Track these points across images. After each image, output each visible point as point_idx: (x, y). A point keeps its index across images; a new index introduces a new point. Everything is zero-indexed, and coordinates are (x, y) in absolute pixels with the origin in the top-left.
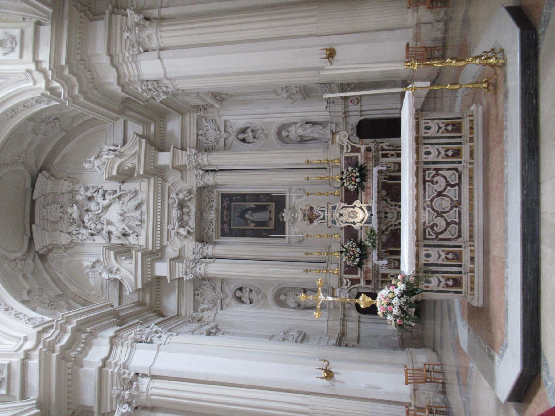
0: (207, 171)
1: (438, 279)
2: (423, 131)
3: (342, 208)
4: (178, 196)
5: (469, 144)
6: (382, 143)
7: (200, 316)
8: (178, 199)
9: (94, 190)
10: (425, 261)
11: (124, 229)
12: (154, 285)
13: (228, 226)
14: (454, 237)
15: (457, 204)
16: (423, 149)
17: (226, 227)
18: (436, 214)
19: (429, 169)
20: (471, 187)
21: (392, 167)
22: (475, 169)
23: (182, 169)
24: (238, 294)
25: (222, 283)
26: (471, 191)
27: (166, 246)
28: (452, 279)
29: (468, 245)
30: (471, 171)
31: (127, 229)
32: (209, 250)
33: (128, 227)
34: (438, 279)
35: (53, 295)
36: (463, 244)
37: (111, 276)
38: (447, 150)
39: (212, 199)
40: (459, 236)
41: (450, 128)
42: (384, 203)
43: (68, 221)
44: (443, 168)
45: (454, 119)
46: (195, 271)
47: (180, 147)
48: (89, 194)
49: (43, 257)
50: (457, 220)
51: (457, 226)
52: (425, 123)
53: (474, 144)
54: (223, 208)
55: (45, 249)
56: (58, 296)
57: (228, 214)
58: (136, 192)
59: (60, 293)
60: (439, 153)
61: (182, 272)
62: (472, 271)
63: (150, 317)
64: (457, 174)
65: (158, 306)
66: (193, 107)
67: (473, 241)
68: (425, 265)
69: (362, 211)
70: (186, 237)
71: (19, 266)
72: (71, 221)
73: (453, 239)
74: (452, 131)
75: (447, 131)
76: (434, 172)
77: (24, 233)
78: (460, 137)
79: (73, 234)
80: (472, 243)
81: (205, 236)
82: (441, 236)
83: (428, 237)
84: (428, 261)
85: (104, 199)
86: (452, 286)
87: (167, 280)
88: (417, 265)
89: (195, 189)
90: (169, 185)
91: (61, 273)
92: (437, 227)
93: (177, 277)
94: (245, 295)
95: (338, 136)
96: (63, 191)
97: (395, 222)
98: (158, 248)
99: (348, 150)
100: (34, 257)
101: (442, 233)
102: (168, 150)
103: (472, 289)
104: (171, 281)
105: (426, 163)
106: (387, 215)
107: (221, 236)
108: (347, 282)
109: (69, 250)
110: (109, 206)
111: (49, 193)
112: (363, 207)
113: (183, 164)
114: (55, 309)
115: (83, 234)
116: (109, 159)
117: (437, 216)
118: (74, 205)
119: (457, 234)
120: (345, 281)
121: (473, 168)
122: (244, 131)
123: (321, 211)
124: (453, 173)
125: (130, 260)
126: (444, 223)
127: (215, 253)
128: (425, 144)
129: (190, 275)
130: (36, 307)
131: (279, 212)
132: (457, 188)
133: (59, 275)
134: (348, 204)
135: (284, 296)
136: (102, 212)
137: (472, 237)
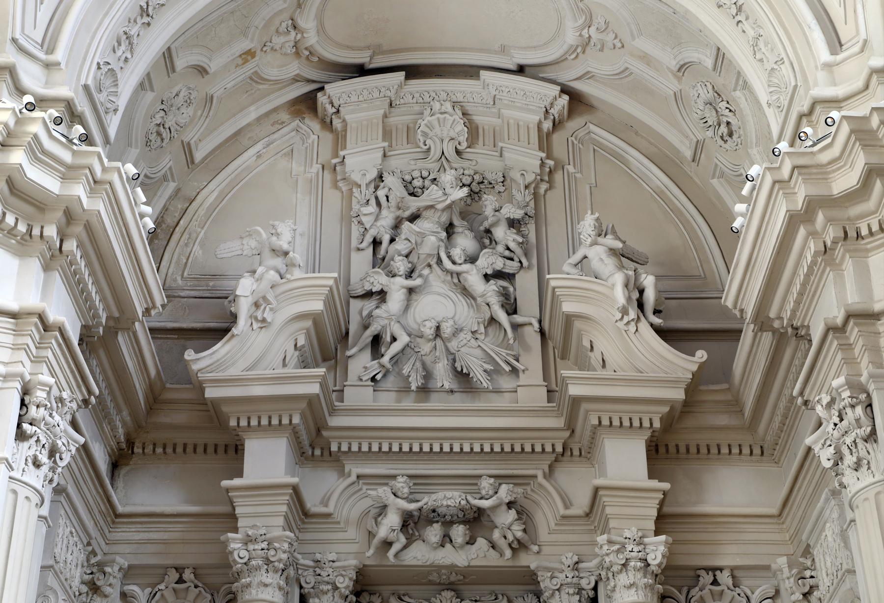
7: (108, 590)
9: (512, 245)
11: (394, 339)
12: (218, 440)
31: (396, 347)
33: (403, 350)
35: (189, 136)
43: (416, 174)
46: (258, 568)
48: (501, 233)
49: (307, 104)
55: (331, 110)
56: (188, 150)
58: (514, 371)
59: (198, 156)
61: (253, 527)
63: (113, 429)
65: (149, 449)
66: (807, 552)
70: (371, 535)
71: (278, 41)
77: (378, 50)
79: (376, 188)
87: (231, 478)
89: (528, 560)
90: (541, 479)
91: (259, 156)
93: (238, 511)
96: (506, 154)
98: (334, 448)
100: (309, 81)
102: (652, 474)
104: (228, 490)
109: (328, 176)
110: (466, 292)
113: (612, 524)
114: (148, 143)
115: (376, 220)
118: (466, 190)
129: (244, 553)
133: (252, 152)
136: (447, 271)
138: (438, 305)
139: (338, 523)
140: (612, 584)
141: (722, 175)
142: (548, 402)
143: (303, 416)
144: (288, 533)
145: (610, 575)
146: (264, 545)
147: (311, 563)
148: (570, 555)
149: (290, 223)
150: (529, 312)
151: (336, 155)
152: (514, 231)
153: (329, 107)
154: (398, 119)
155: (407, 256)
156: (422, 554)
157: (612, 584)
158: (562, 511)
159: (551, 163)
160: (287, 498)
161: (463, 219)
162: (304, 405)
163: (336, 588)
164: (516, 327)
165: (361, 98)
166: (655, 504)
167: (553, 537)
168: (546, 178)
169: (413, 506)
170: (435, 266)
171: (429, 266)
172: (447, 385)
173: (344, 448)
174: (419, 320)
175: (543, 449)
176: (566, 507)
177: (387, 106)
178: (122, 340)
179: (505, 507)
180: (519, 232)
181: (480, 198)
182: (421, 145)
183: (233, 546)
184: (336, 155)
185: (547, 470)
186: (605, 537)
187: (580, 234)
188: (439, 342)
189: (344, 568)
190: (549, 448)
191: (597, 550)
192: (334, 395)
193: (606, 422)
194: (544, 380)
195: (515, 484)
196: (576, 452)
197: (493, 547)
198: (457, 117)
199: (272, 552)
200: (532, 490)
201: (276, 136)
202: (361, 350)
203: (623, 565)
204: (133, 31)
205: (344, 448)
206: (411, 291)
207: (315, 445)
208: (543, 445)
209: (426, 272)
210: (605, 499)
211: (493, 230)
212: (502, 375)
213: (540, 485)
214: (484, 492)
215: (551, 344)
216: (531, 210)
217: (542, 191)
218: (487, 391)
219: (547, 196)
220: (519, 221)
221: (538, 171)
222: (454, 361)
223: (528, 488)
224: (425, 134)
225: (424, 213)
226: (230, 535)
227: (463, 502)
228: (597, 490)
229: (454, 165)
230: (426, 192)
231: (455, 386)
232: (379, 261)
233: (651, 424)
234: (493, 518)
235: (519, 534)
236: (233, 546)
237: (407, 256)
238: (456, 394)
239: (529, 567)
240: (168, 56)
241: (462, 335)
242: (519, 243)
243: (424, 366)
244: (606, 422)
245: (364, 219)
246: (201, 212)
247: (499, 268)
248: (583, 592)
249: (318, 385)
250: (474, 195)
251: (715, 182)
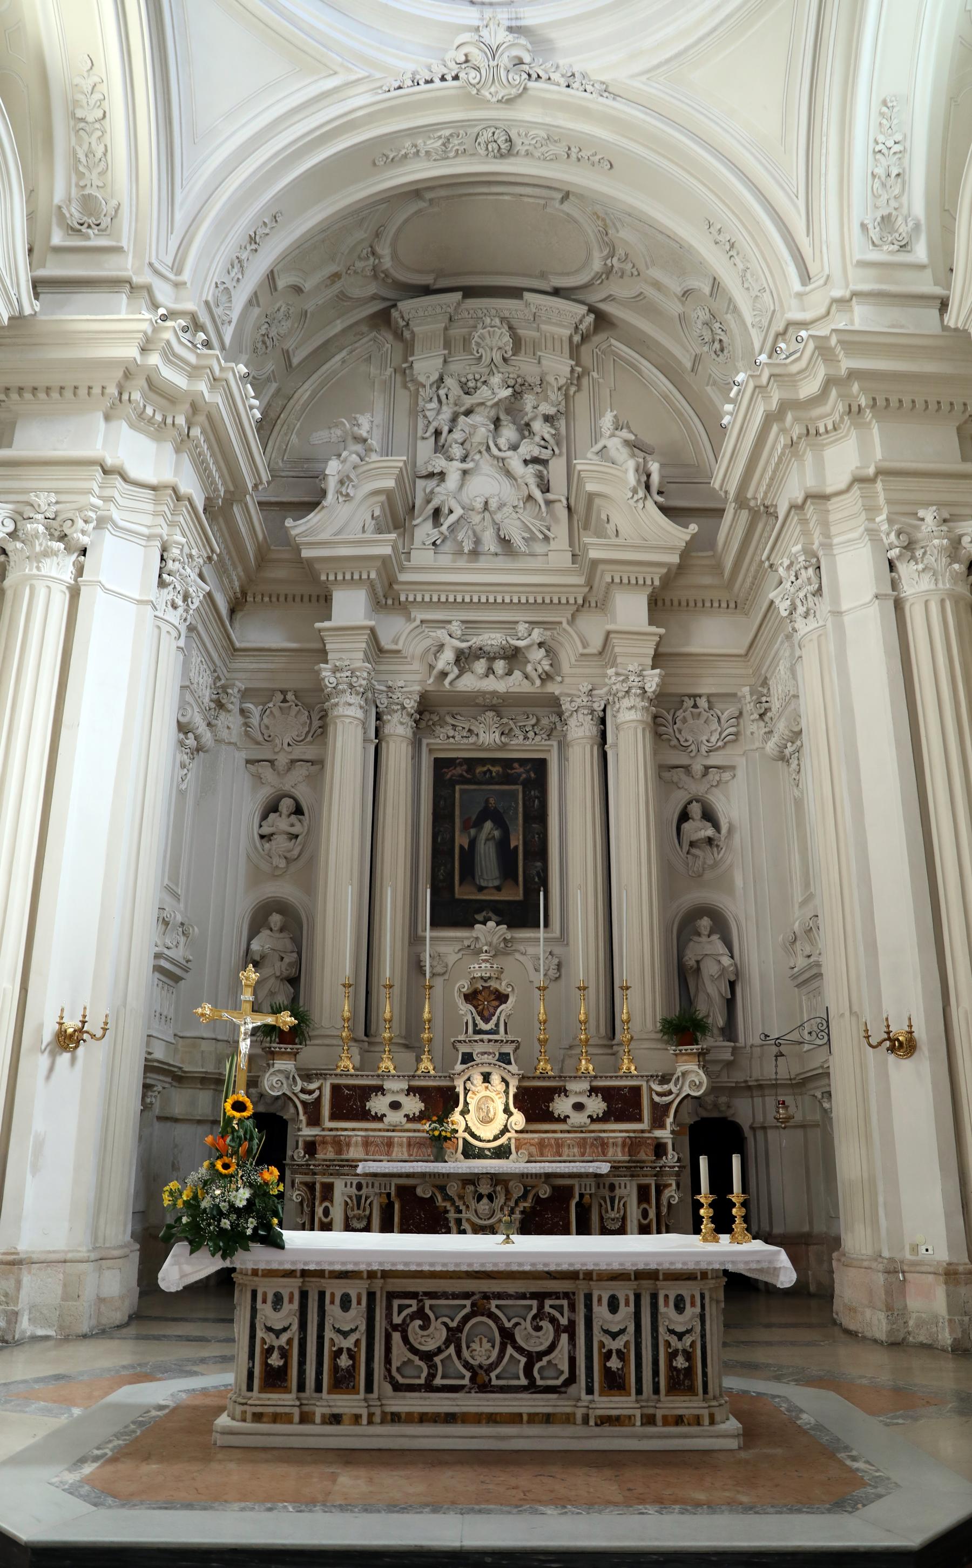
0: (603, 721)
1: (285, 1329)
2: (671, 1290)
3: (504, 1080)
5: (638, 1413)
6: (678, 1185)
7: (230, 706)
8: (528, 647)
9: (547, 437)
10: (333, 1295)
11: (451, 512)
12: (311, 592)
13: (461, 775)
14: (394, 1373)
15: (479, 1381)
16: (624, 1292)
17: (459, 771)
18: (453, 1324)
19: (572, 1307)
20: (525, 1418)
21: (613, 1215)
22: (570, 1430)
24: (286, 805)
25: (313, 763)
26: (515, 1419)
27: (409, 619)
28: (286, 1364)
29: (372, 1410)
30: (568, 1419)
31: (452, 518)
32: (399, 728)
33: (458, 521)
34: (285, 1329)
35: (289, 344)
36: (375, 1395)
37: (332, 485)
38: (621, 1355)
39: (531, 734)
40: (397, 1387)
41: (680, 1362)
42: (517, 1192)
43: (470, 377)
44: (574, 1346)
45: (705, 1374)
46: (344, 691)
47: (661, 650)
50: (438, 1381)
51: (422, 1381)
52: (693, 1297)
53: (638, 1429)
54: (507, 763)
55: (402, 323)
56: (287, 355)
57: (492, 777)
58: (546, 538)
59: (295, 361)
60: (614, 1336)
61: (340, 659)
62: (305, 1418)
63: (231, 581)
64: (558, 1382)
65: (258, 598)
67: (383, 1422)
68: (322, 1295)
69: (497, 1132)
70: (431, 667)
71: (360, 265)
72: (471, 384)
73: (389, 1371)
74: (671, 1368)
75: (672, 1356)
76: (564, 1321)
77: (440, 274)
78: (656, 1391)
79: (438, 388)
80: (377, 1419)
81: (436, 718)
82: (396, 1336)
83: (396, 1303)
84: (332, 1302)
85: (526, 462)
86: (267, 1364)
88: (320, 1274)
89: (553, 688)
90: (565, 625)
91: (343, 361)
92: (423, 1328)
93: (328, 647)
94: (280, 823)
95: (696, 1068)
96: (544, 362)
97: (468, 1220)
98: (403, 598)
99: (660, 1094)
101: (406, 1340)
103: (258, 1417)
104: (320, 631)
105: (588, 1297)
106: (485, 1200)
107: (436, 760)
108: (310, 1092)
109: (399, 378)
110: (508, 474)
111: (538, 329)
112: (507, 1135)
113: (619, 660)
114: (255, 350)
115: (438, 414)
116: (626, 471)
117: (449, 1329)
118: (510, 390)
119: (401, 1380)
120: (312, 1086)
121: (575, 1424)
122: (709, 816)
123: (497, 1025)
124: (562, 1372)
125: (372, 528)
126: (430, 1346)
127: (392, 746)
128: (638, 1297)
129: (332, 680)
130: (259, 306)
131: (497, 912)
132: (523, 1381)
133: (338, 357)
134: (515, 1096)
135: (279, 924)
136: (494, 457)
137: (393, 1421)
138: (486, 484)
139: (406, 657)
140: (617, 706)
141: (715, 383)
143: (378, 573)
144: (367, 664)
145: (616, 699)
146: (349, 674)
147: (385, 689)
149: (368, 415)
150: (559, 490)
151: (406, 361)
153: (400, 320)
154: (457, 332)
155: (462, 444)
156: (470, 683)
157: (617, 706)
158: (581, 650)
159: (579, 369)
160: (366, 637)
161: (508, 414)
162: (379, 564)
163: (404, 708)
164: (548, 503)
165: (426, 314)
166: (652, 645)
167: (574, 671)
168: (575, 382)
169: (464, 645)
170: (484, 452)
171: (480, 452)
172: (493, 549)
173: (411, 599)
174: (471, 496)
175: (568, 602)
176: (584, 647)
177: (447, 321)
178: (236, 509)
179: (536, 647)
180: (552, 426)
181: (522, 398)
182: (475, 353)
183: (324, 674)
184: (406, 361)
185: (570, 618)
186: (613, 670)
187: (601, 428)
188: (487, 514)
189: (410, 693)
190: (572, 601)
191: (607, 680)
192: (403, 556)
193: (617, 580)
196: (593, 604)
197: (526, 678)
198: (504, 330)
199: (355, 679)
201: (357, 345)
202: (424, 520)
203: (627, 692)
204: (244, 256)
205: (411, 599)
206: (465, 472)
207: (388, 596)
209: (477, 457)
210: (615, 641)
211: (532, 424)
213: (564, 630)
214: (520, 635)
215: (575, 517)
216: (562, 408)
217: (572, 393)
218: (525, 554)
220: (552, 417)
221: (569, 376)
222: (499, 529)
223: (555, 632)
224: (478, 344)
225: (477, 409)
226: (322, 665)
227: (504, 642)
228: (608, 633)
229: (501, 370)
230: (478, 392)
231: (499, 550)
232: (440, 448)
234: (527, 655)
235: (547, 668)
236: (324, 674)
237: (462, 444)
238: (501, 557)
240: (271, 277)
241: (505, 509)
242: (553, 435)
243: (474, 533)
244: (617, 580)
245: (428, 413)
246: (298, 407)
249: (390, 548)
250: (517, 395)
251: (709, 389)
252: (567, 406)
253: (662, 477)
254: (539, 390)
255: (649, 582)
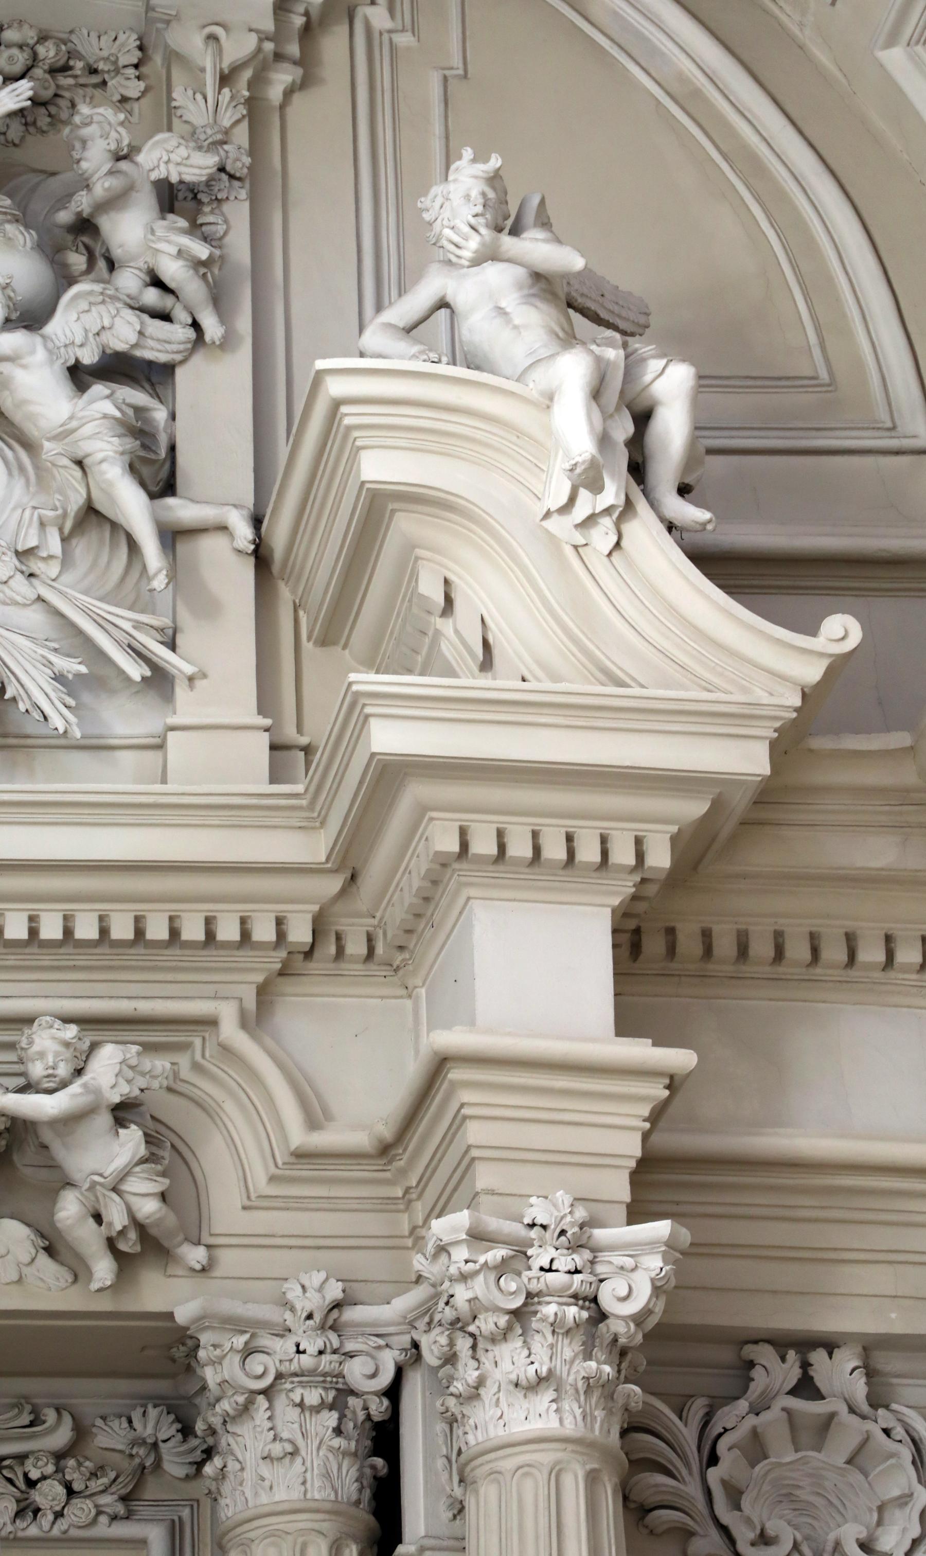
0: (385, 1438)
4: (105, 1120)
9: (173, 270)
23: (415, 1145)
48: (133, 230)
58: (160, 681)
90: (230, 1030)
142: (273, 780)
148: (317, 1278)
152: (183, 223)
157: (472, 1375)
158: (298, 1136)
164: (173, 536)
167: (262, 1221)
168: (294, 49)
175: (245, 935)
176: (313, 1124)
180: (195, 228)
190: (264, 932)
194: (262, 710)
195: (149, 1048)
196: (356, 947)
200: (196, 1067)
208: (243, 921)
211: (105, 223)
212: (112, 692)
213: (226, 1050)
217: (275, 93)
219: (290, 111)
221: (269, 25)
223: (184, 1061)
233: (640, 856)
239: (170, 1316)
242: (199, 265)
247: (121, 347)
248: (352, 1401)
252: (256, 147)
253: (698, 428)
254: (134, 88)
255: (623, 855)
